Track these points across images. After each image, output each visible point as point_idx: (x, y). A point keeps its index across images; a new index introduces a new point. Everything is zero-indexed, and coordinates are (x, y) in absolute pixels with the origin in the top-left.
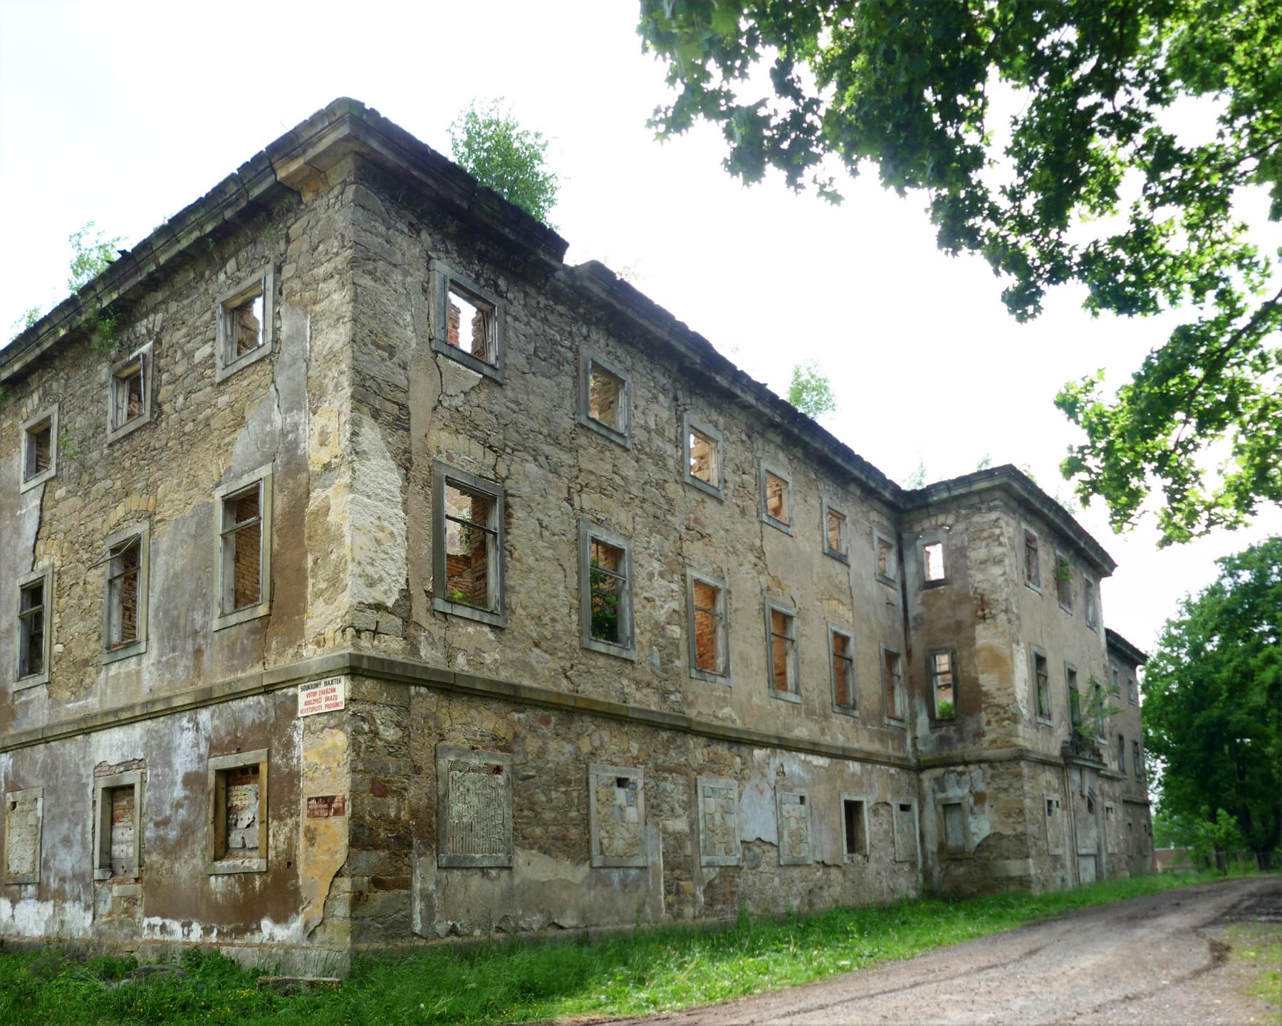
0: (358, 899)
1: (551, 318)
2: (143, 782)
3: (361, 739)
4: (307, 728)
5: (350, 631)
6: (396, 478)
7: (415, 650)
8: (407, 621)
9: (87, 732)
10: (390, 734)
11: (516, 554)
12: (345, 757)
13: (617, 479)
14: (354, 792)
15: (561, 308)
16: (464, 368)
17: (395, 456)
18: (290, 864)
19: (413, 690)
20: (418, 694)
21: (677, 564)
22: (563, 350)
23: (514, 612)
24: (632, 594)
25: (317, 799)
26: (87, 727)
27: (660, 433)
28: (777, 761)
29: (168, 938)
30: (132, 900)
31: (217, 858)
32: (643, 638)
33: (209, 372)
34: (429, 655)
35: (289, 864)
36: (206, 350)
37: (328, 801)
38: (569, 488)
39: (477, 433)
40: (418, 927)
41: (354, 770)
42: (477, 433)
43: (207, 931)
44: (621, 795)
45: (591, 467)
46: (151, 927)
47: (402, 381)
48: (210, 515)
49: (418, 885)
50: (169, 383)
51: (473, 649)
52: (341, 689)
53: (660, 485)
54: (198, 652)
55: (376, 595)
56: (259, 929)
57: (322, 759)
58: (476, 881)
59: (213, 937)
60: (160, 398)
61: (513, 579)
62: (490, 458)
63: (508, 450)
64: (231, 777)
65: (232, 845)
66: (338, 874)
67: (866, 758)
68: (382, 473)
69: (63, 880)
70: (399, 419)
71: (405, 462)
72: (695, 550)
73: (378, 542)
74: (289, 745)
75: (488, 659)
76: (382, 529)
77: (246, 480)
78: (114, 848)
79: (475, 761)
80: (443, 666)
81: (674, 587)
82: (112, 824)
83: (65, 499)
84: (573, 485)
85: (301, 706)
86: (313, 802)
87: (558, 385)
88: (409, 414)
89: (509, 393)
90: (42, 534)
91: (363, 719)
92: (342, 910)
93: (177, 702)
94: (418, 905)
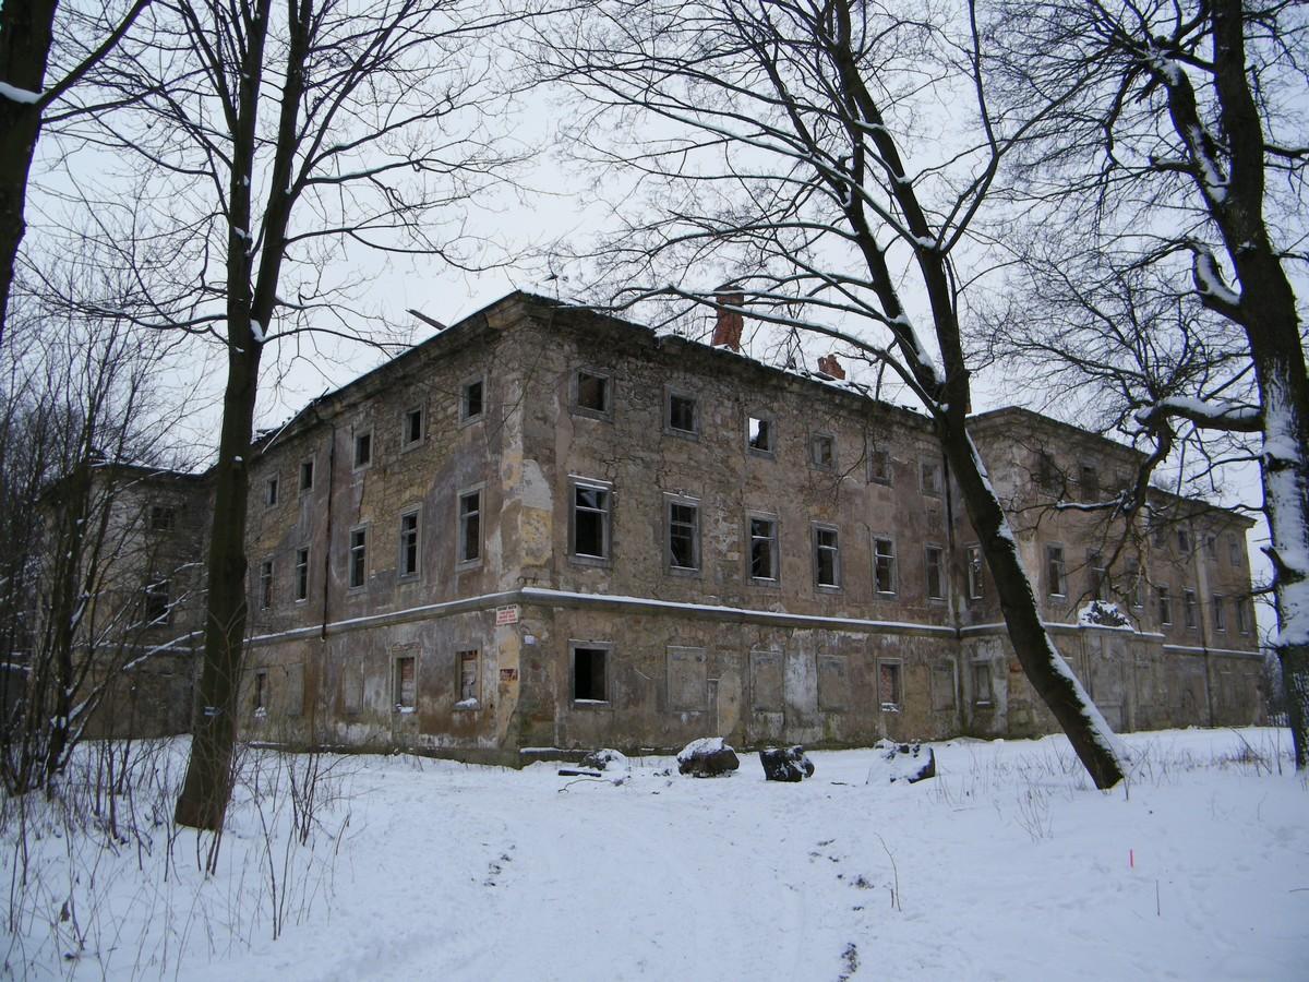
1: (645, 373)
13: (692, 463)
15: (651, 365)
21: (736, 510)
24: (701, 535)
26: (389, 623)
27: (725, 425)
32: (709, 560)
37: (510, 671)
45: (673, 458)
46: (423, 740)
47: (552, 436)
48: (454, 506)
52: (516, 612)
53: (725, 461)
61: (618, 537)
72: (753, 498)
78: (404, 694)
81: (735, 526)
89: (617, 426)
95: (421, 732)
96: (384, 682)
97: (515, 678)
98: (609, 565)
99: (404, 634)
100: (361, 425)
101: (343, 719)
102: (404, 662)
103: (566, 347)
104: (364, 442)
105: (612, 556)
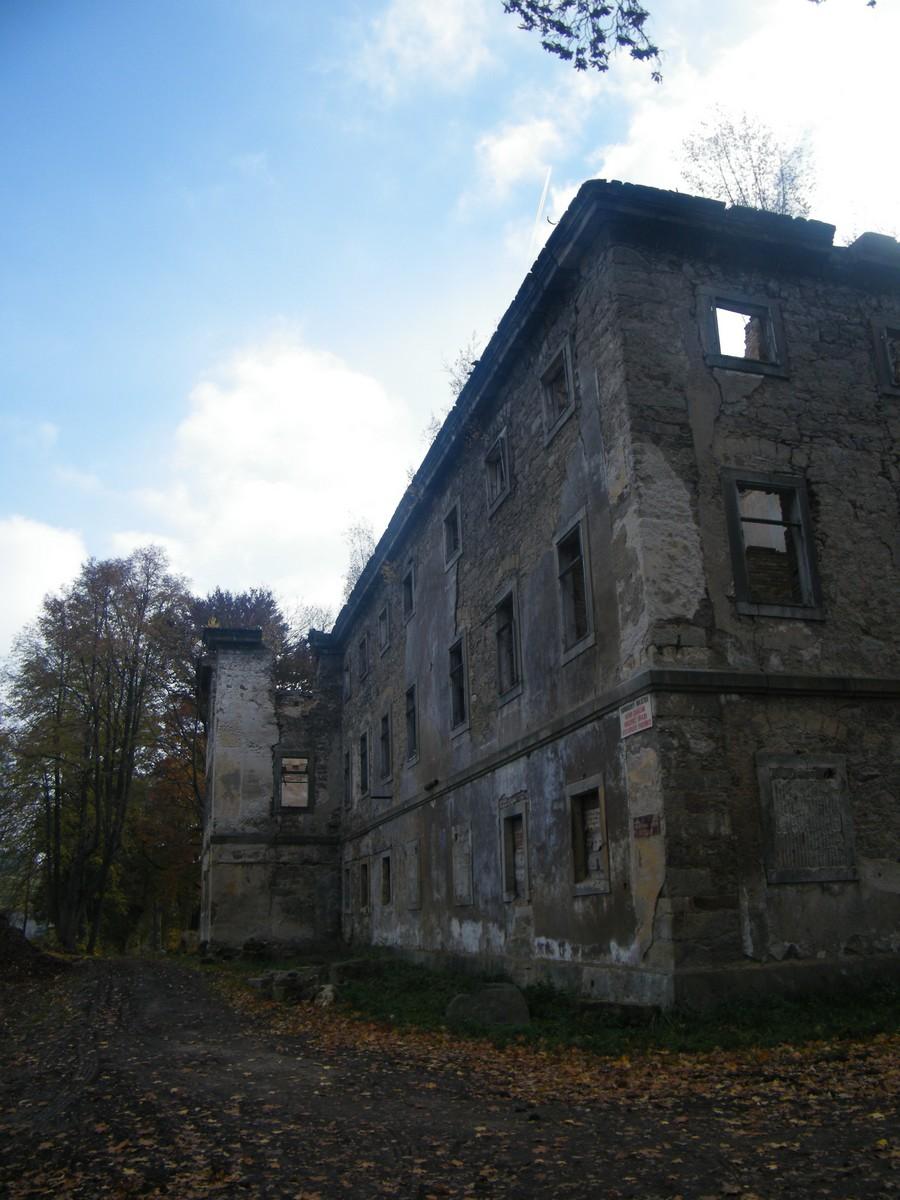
0: (678, 920)
2: (527, 811)
3: (672, 754)
4: (629, 747)
5: (652, 649)
6: (685, 494)
7: (719, 656)
8: (711, 630)
9: (493, 768)
10: (702, 746)
11: (829, 542)
12: (656, 774)
14: (666, 809)
16: (743, 374)
17: (680, 473)
18: (626, 885)
19: (723, 698)
20: (729, 703)
22: (852, 328)
23: (834, 602)
25: (640, 819)
26: (492, 766)
29: (551, 957)
30: (527, 920)
31: (577, 880)
33: (541, 439)
34: (737, 660)
35: (625, 885)
36: (538, 421)
38: (883, 461)
39: (766, 432)
41: (665, 787)
42: (766, 432)
43: (575, 951)
49: (745, 903)
50: (519, 457)
52: (647, 708)
54: (554, 686)
55: (676, 609)
56: (608, 951)
57: (642, 778)
59: (579, 958)
60: (515, 472)
62: (785, 452)
63: (806, 439)
64: (587, 800)
65: (591, 868)
66: (660, 895)
68: (672, 492)
69: (486, 902)
70: (681, 437)
71: (692, 477)
73: (672, 558)
74: (617, 768)
75: (806, 655)
76: (674, 545)
77: (571, 524)
82: (514, 850)
83: (470, 571)
84: (887, 457)
85: (623, 728)
86: (638, 822)
87: (852, 363)
88: (690, 430)
90: (460, 603)
91: (672, 735)
92: (666, 932)
93: (543, 735)
95: (538, 934)
96: (493, 856)
97: (656, 831)
98: (817, 616)
99: (509, 779)
100: (449, 505)
101: (456, 916)
102: (514, 821)
103: (686, 267)
104: (451, 521)
105: (820, 598)
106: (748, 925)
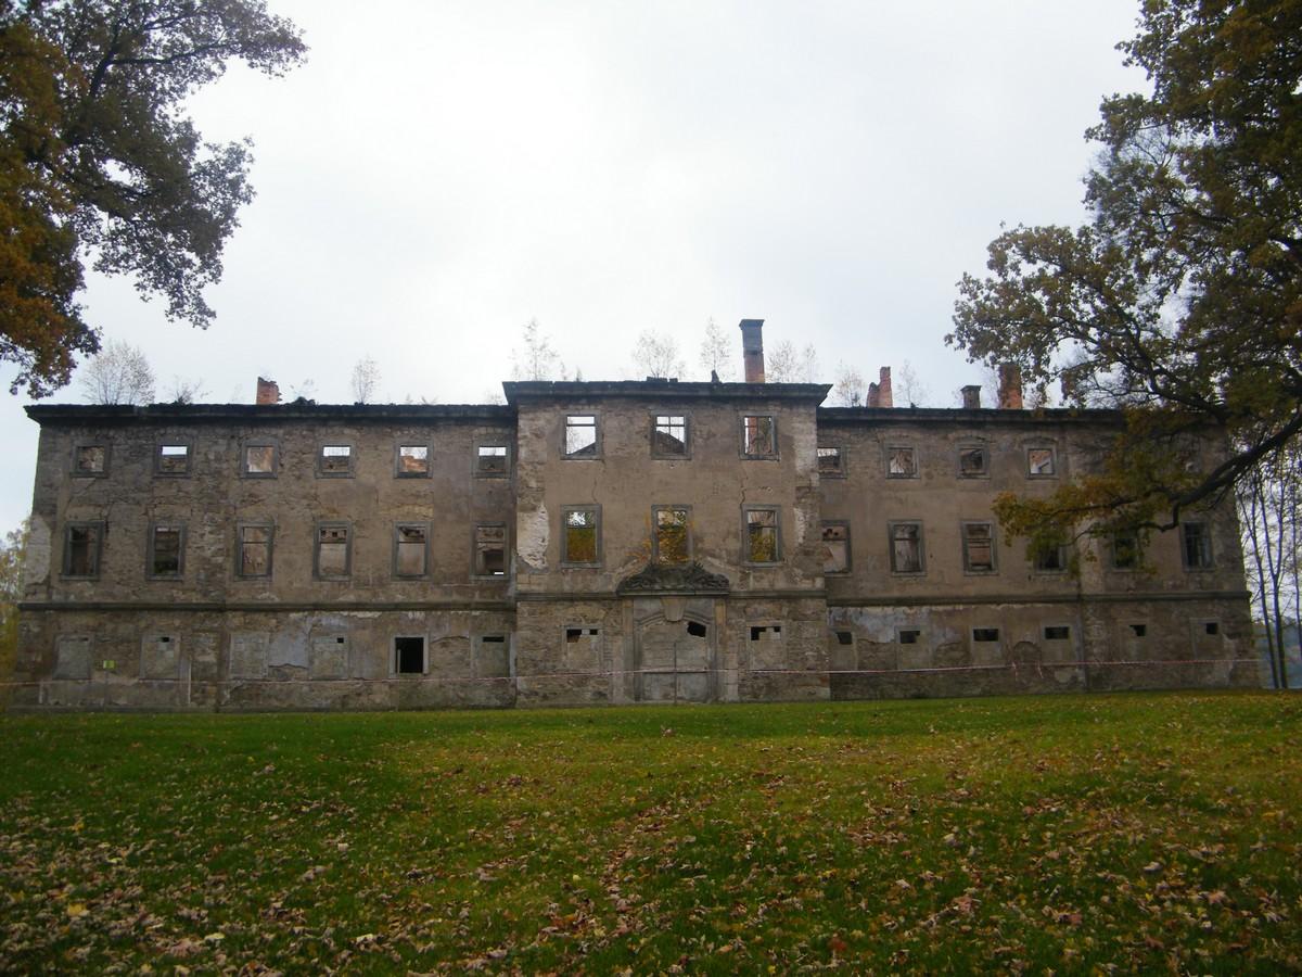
7: (50, 597)
10: (36, 630)
17: (49, 525)
28: (315, 618)
34: (56, 598)
40: (41, 700)
44: (163, 646)
51: (84, 590)
55: (35, 580)
58: (70, 684)
67: (428, 607)
71: (53, 527)
75: (86, 594)
79: (74, 637)
80: (63, 601)
94: (41, 693)
106: (41, 693)
